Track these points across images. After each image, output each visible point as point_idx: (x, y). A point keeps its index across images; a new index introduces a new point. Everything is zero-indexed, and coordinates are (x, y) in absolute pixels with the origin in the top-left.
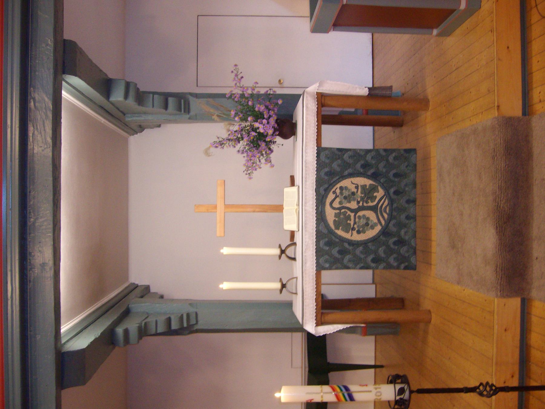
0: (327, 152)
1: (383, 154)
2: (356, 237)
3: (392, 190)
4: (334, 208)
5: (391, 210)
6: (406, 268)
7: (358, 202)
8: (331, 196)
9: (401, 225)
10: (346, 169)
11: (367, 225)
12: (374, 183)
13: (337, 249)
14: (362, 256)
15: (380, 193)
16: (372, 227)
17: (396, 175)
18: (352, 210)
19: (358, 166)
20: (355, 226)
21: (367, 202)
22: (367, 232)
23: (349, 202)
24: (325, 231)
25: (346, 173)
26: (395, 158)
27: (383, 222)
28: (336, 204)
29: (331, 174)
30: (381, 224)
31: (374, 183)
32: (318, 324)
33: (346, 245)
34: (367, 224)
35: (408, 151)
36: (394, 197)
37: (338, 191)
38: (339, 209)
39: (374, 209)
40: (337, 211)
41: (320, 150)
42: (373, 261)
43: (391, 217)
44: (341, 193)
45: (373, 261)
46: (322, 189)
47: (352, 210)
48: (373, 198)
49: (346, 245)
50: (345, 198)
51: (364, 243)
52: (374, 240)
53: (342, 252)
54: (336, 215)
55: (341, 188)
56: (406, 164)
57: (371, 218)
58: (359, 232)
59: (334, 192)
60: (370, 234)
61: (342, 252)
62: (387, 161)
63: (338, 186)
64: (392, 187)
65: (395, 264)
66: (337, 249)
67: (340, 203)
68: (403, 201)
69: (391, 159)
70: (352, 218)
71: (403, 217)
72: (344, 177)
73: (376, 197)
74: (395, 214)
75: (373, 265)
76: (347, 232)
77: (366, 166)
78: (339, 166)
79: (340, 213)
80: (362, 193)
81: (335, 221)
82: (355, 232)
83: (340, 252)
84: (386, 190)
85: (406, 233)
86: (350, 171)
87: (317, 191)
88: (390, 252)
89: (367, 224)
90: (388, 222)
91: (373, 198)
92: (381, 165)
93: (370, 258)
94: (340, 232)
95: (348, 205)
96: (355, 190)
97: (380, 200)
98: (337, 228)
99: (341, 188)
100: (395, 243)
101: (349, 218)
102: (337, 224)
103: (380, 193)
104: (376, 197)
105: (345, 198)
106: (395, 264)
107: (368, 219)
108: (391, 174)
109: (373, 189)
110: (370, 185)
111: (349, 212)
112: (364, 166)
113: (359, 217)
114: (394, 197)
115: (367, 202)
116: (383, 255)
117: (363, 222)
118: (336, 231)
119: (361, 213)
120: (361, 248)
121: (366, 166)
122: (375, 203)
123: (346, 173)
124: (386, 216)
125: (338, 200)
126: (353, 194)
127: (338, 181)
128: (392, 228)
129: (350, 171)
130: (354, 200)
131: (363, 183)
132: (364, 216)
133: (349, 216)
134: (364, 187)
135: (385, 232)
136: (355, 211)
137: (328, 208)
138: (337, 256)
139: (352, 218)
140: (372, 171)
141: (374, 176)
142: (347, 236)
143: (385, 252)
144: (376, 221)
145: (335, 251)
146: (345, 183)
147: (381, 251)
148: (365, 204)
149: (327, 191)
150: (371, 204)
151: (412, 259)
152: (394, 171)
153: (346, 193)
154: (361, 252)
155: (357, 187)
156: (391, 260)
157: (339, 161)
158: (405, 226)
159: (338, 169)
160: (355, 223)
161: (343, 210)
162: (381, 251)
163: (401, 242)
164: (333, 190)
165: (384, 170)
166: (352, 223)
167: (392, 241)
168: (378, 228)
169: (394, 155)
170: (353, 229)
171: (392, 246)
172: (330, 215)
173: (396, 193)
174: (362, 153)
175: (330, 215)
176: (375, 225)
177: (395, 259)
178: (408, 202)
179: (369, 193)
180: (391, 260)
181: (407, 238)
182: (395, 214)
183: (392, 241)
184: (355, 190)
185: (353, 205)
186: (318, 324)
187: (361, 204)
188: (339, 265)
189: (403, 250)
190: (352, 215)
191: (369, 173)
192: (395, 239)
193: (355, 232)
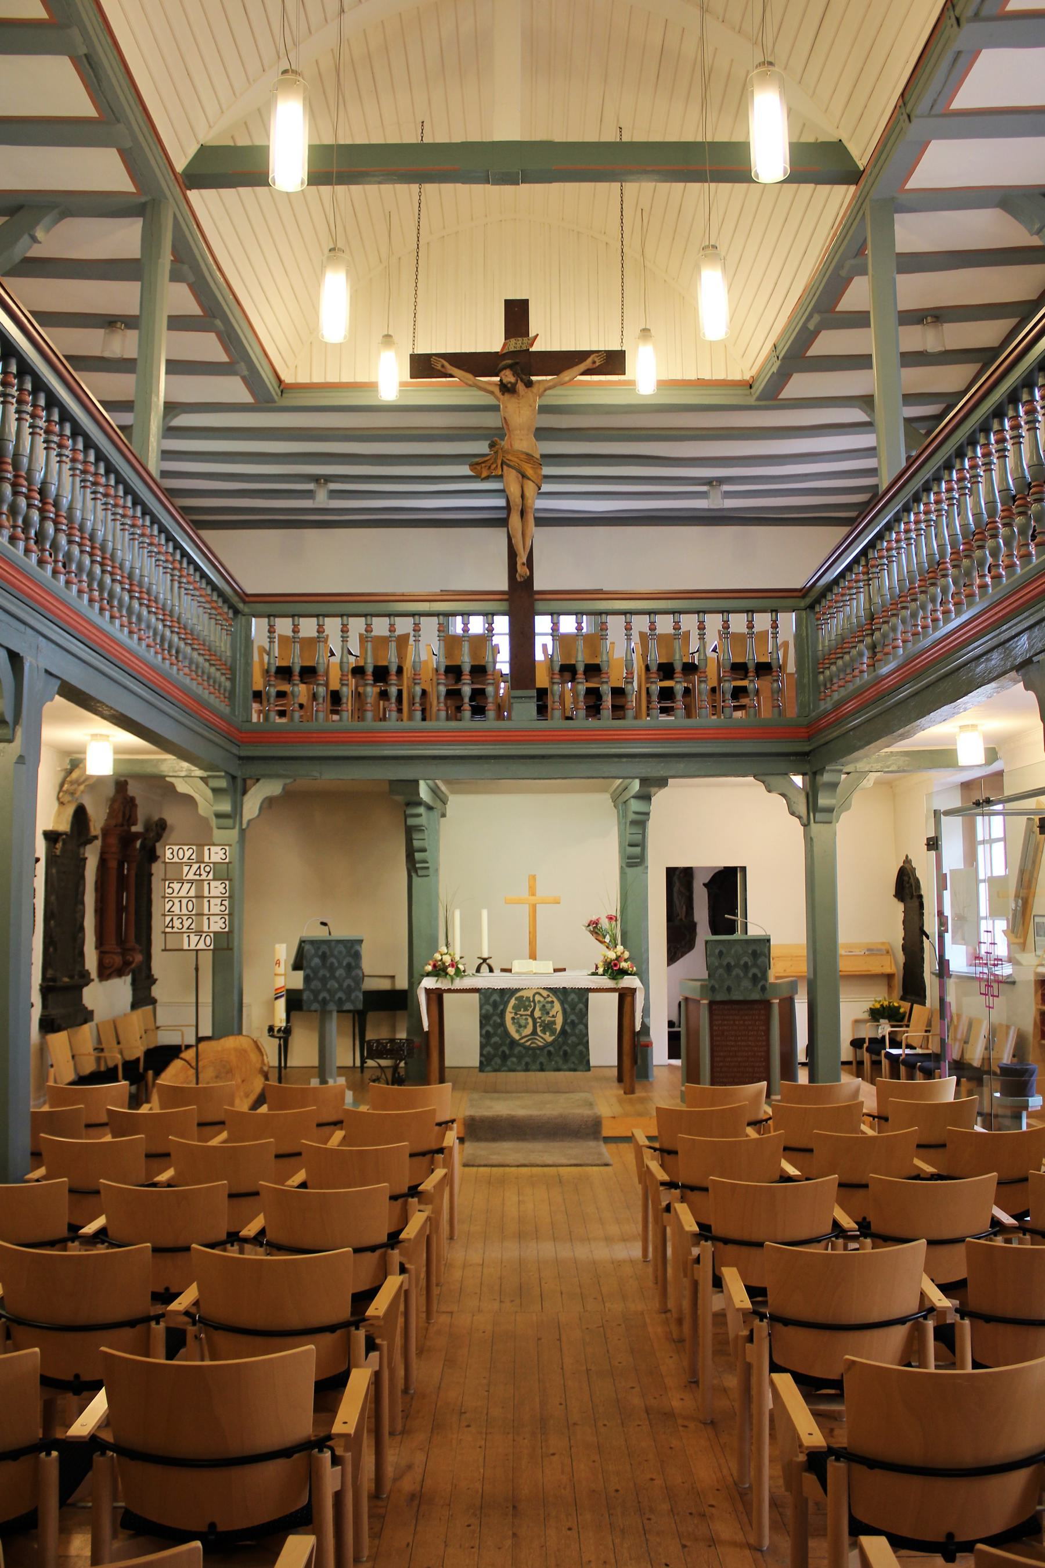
2: (509, 1016)
3: (551, 1049)
4: (534, 996)
5: (534, 1049)
7: (540, 1018)
9: (520, 1057)
10: (569, 1006)
11: (520, 1027)
13: (498, 999)
14: (491, 1022)
15: (549, 1038)
16: (517, 1031)
17: (565, 1053)
19: (573, 1017)
21: (540, 1026)
23: (540, 1010)
25: (566, 1006)
26: (581, 1052)
27: (523, 1041)
28: (538, 997)
30: (520, 1039)
33: (501, 1007)
34: (520, 1026)
36: (546, 1051)
37: (549, 999)
38: (534, 1001)
39: (534, 1032)
42: (488, 1032)
43: (528, 1048)
45: (488, 1032)
48: (544, 1031)
49: (501, 1007)
50: (544, 1006)
51: (503, 1024)
52: (506, 1033)
53: (495, 1005)
54: (528, 998)
55: (552, 1002)
56: (576, 1062)
58: (513, 1018)
59: (548, 996)
60: (512, 1029)
61: (495, 1005)
62: (579, 1044)
63: (555, 999)
64: (554, 1047)
65: (485, 1052)
67: (539, 1002)
68: (542, 1059)
71: (527, 1059)
72: (562, 1004)
73: (545, 1034)
74: (530, 1052)
75: (484, 1032)
76: (513, 1008)
78: (573, 999)
79: (530, 1001)
82: (513, 1015)
83: (495, 1002)
84: (552, 1043)
85: (513, 1063)
86: (568, 1010)
88: (496, 1046)
89: (520, 1026)
90: (522, 1045)
91: (544, 1031)
93: (489, 1028)
94: (513, 1002)
95: (537, 1009)
96: (551, 1015)
97: (542, 1038)
98: (516, 999)
99: (552, 1002)
100: (503, 1052)
101: (526, 1010)
104: (545, 1034)
105: (544, 1006)
106: (485, 1052)
107: (525, 1027)
108: (566, 1048)
109: (553, 1032)
110: (556, 1029)
112: (573, 1022)
113: (527, 1019)
114: (546, 1051)
115: (540, 1026)
117: (523, 1022)
118: (514, 999)
119: (530, 1020)
120: (499, 1021)
122: (539, 1033)
125: (542, 999)
126: (548, 1013)
127: (559, 999)
128: (517, 1050)
129: (568, 1010)
130: (542, 1014)
132: (528, 1023)
133: (528, 1010)
134: (554, 1023)
135: (513, 1043)
136: (532, 1015)
140: (569, 1030)
141: (563, 1032)
142: (510, 1008)
143: (495, 1043)
144: (523, 1035)
146: (557, 1006)
147: (495, 1039)
150: (539, 1029)
151: (489, 1068)
152: (569, 1051)
153: (548, 1006)
154: (495, 1022)
155: (553, 1016)
156: (489, 1049)
157: (576, 1000)
158: (519, 1062)
159: (569, 999)
160: (521, 1015)
161: (532, 1004)
162: (495, 1039)
163: (504, 1057)
165: (569, 1042)
166: (522, 1012)
167: (505, 1049)
168: (516, 1036)
169: (584, 1050)
170: (516, 1014)
171: (501, 1049)
173: (549, 1053)
174: (584, 1021)
176: (520, 1034)
177: (489, 1052)
178: (541, 1064)
179: (548, 1027)
180: (489, 1049)
181: (509, 1063)
182: (530, 1052)
183: (505, 1049)
184: (551, 1015)
187: (538, 1020)
188: (483, 1002)
189: (498, 1060)
190: (529, 1013)
191: (567, 1028)
192: (507, 1052)
193: (513, 1015)
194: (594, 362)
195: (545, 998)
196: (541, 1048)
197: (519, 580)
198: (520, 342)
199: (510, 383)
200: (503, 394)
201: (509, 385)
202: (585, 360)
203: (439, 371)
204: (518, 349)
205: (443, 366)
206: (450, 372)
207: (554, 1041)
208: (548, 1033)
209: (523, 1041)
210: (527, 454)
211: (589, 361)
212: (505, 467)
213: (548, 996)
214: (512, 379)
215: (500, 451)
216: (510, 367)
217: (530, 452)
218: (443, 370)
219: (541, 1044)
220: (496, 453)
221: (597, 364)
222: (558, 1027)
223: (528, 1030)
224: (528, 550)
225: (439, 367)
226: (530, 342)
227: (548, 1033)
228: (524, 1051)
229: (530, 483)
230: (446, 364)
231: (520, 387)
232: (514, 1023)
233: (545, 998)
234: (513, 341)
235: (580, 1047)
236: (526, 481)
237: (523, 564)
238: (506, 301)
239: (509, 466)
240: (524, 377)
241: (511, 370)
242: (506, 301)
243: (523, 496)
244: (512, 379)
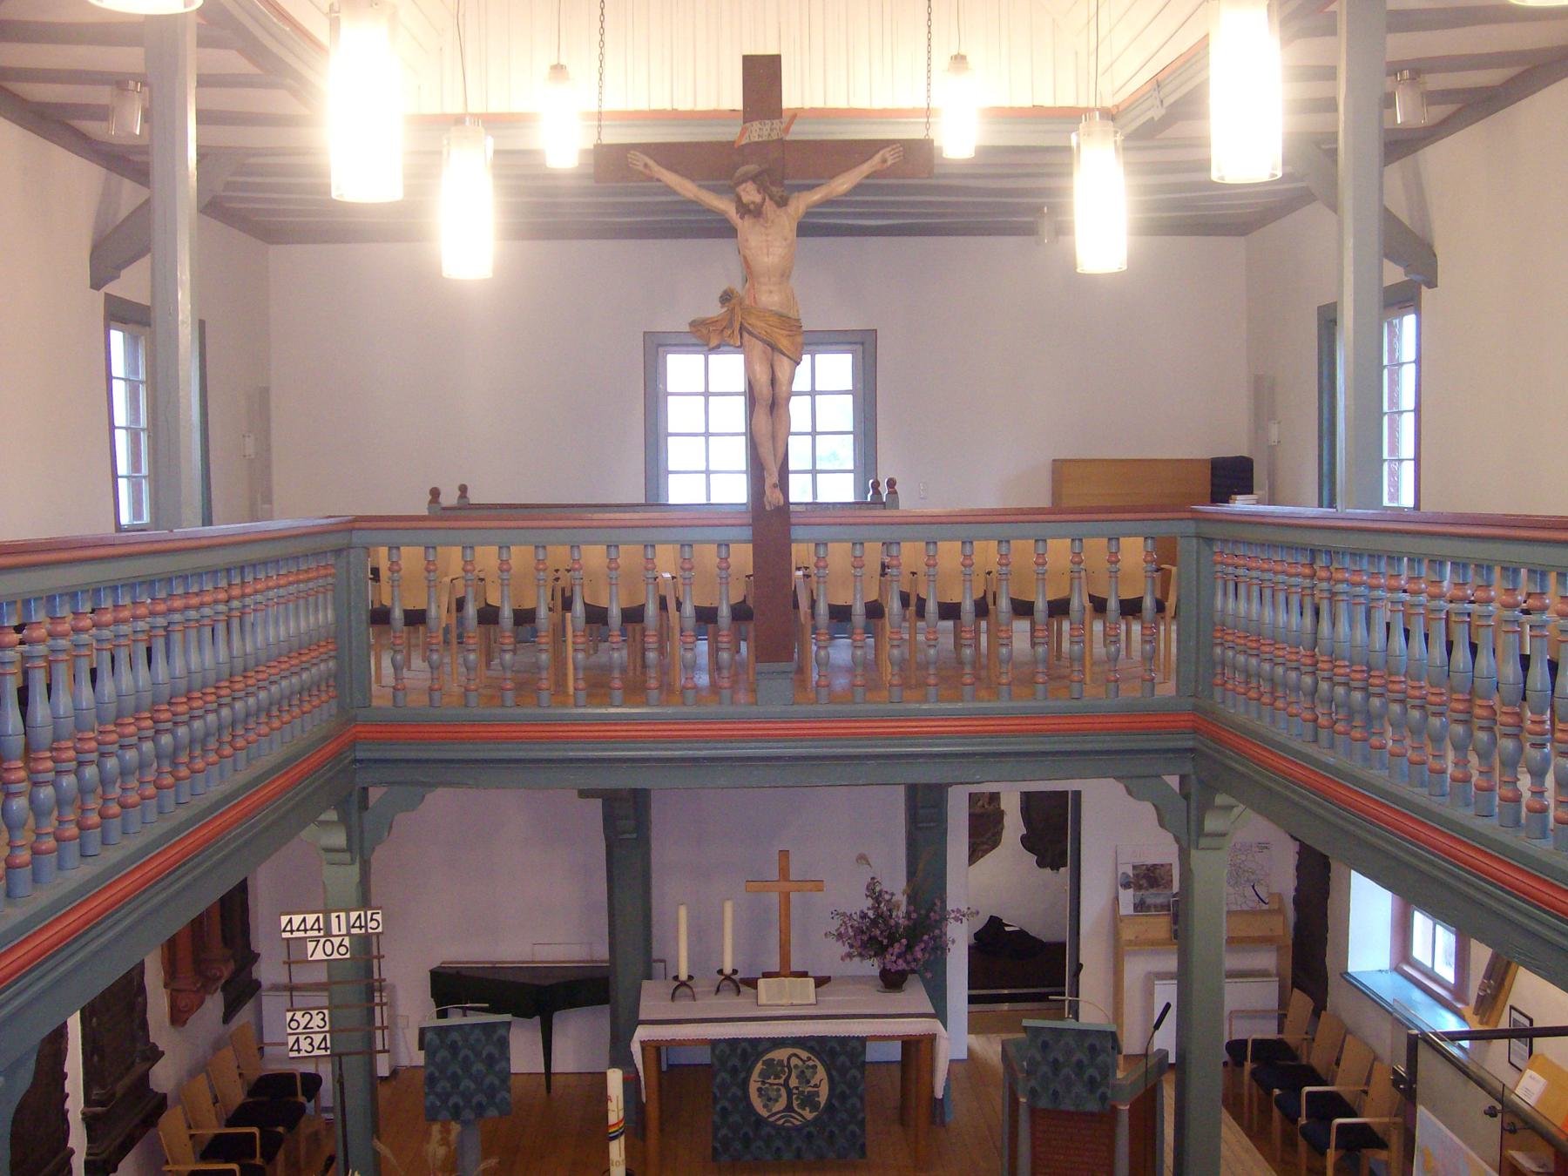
0: (860, 1049)
1: (860, 1116)
3: (811, 1129)
4: (789, 1059)
5: (788, 1129)
6: (715, 1149)
7: (797, 1088)
8: (804, 1055)
11: (769, 1100)
12: (822, 1106)
13: (739, 1064)
15: (809, 1115)
16: (765, 1106)
18: (787, 1081)
20: (767, 1085)
21: (797, 1098)
22: (759, 1100)
24: (760, 1048)
25: (834, 1073)
26: (853, 1133)
27: (772, 1119)
28: (794, 1061)
29: (833, 1054)
30: (769, 1117)
31: (822, 1106)
32: (641, 1042)
33: (742, 1075)
34: (770, 1099)
35: (863, 1146)
37: (811, 1063)
39: (789, 1108)
40: (786, 1063)
41: (862, 1041)
43: (782, 1127)
44: (808, 1067)
45: (724, 1109)
46: (813, 1043)
47: (787, 1081)
48: (802, 1106)
49: (742, 1075)
50: (803, 1072)
51: (746, 1097)
52: (749, 1105)
53: (734, 1071)
57: (777, 1104)
58: (759, 1090)
59: (809, 1059)
60: (757, 1103)
61: (734, 1071)
63: (818, 1063)
66: (739, 1064)
67: (796, 1066)
69: (852, 1127)
70: (777, 1081)
73: (804, 1109)
77: (843, 1097)
80: (809, 1092)
81: (773, 1060)
82: (759, 1085)
84: (815, 1121)
87: (812, 1038)
89: (770, 1099)
90: (773, 1125)
92: (845, 1116)
93: (727, 1104)
94: (759, 1066)
96: (812, 1084)
98: (765, 1063)
99: (815, 1067)
102: (769, 1063)
103: (809, 1115)
104: (804, 1109)
105: (803, 1072)
107: (776, 1101)
111: (784, 1077)
115: (797, 1098)
116: (731, 1120)
117: (773, 1094)
118: (761, 1062)
119: (783, 1092)
120: (739, 1093)
121: (843, 1097)
122: (796, 1109)
123: (834, 1073)
124: (781, 1122)
125: (800, 1063)
126: (808, 1082)
127: (821, 1060)
128: (766, 1130)
131: (821, 1093)
132: (780, 1096)
133: (780, 1078)
135: (760, 1121)
137: (790, 1051)
138: (730, 1064)
139: (777, 1081)
140: (837, 1104)
141: (830, 1106)
144: (774, 1110)
145: (735, 1061)
146: (821, 1073)
147: (735, 1118)
148: (794, 1097)
149: (811, 1050)
150: (795, 1103)
153: (808, 1073)
155: (816, 1086)
156: (724, 1131)
157: (848, 1064)
160: (771, 1084)
161: (786, 1069)
162: (735, 1118)
163: (747, 1141)
164: (813, 1057)
168: (764, 1113)
170: (763, 1083)
172: (780, 1054)
173: (810, 1136)
175: (780, 1054)
179: (809, 1101)
180: (724, 1131)
184: (812, 1084)
185: (793, 1082)
186: (641, 1042)
187: (795, 1091)
189: (738, 1145)
190: (782, 1081)
191: (834, 1101)
193: (759, 1085)
194: (884, 161)
195: (804, 1061)
196: (798, 1129)
197: (768, 508)
198: (768, 127)
199: (753, 203)
200: (742, 217)
201: (752, 207)
202: (871, 157)
203: (641, 172)
204: (765, 138)
205: (646, 165)
206: (657, 176)
207: (816, 1118)
208: (808, 1109)
209: (772, 1119)
210: (781, 316)
211: (877, 158)
212: (746, 335)
213: (809, 1059)
214: (757, 198)
215: (737, 309)
216: (754, 178)
217: (785, 312)
218: (647, 171)
219: (799, 1123)
220: (732, 311)
221: (889, 163)
222: (823, 1098)
223: (781, 1104)
224: (780, 462)
225: (641, 168)
226: (783, 126)
227: (808, 1109)
228: (773, 1132)
229: (785, 359)
230: (651, 163)
231: (769, 207)
232: (760, 1095)
233: (804, 1061)
234: (756, 125)
235: (852, 1127)
236: (777, 356)
237: (775, 486)
238: (746, 58)
239: (750, 333)
240: (774, 189)
241: (754, 182)
242: (746, 58)
243: (773, 381)
244: (757, 198)
